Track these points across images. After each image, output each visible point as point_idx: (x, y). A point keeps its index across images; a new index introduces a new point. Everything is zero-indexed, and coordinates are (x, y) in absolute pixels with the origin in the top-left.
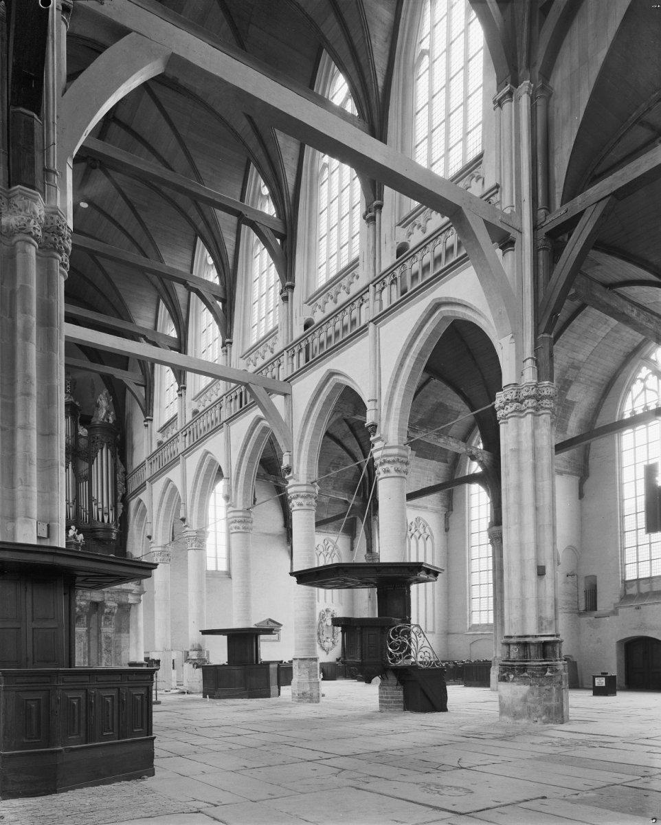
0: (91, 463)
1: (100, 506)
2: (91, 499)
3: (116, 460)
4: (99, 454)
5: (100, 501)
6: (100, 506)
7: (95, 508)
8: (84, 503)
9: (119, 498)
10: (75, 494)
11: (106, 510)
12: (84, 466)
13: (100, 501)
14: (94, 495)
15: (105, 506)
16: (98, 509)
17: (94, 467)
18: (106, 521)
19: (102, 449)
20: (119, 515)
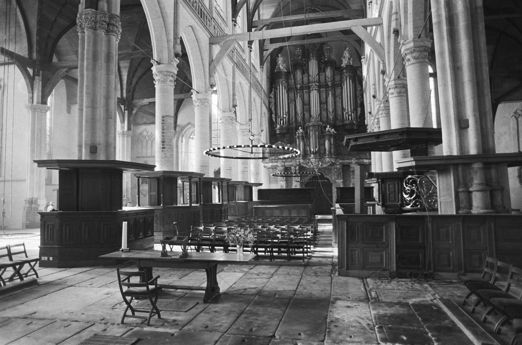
0: (342, 89)
1: (347, 111)
2: (343, 109)
3: (356, 84)
4: (345, 83)
5: (347, 108)
6: (347, 111)
7: (345, 113)
8: (339, 112)
9: (359, 105)
10: (334, 107)
11: (350, 113)
12: (338, 91)
13: (347, 108)
14: (344, 106)
15: (349, 111)
16: (346, 113)
17: (343, 90)
18: (350, 119)
19: (347, 80)
20: (359, 114)
